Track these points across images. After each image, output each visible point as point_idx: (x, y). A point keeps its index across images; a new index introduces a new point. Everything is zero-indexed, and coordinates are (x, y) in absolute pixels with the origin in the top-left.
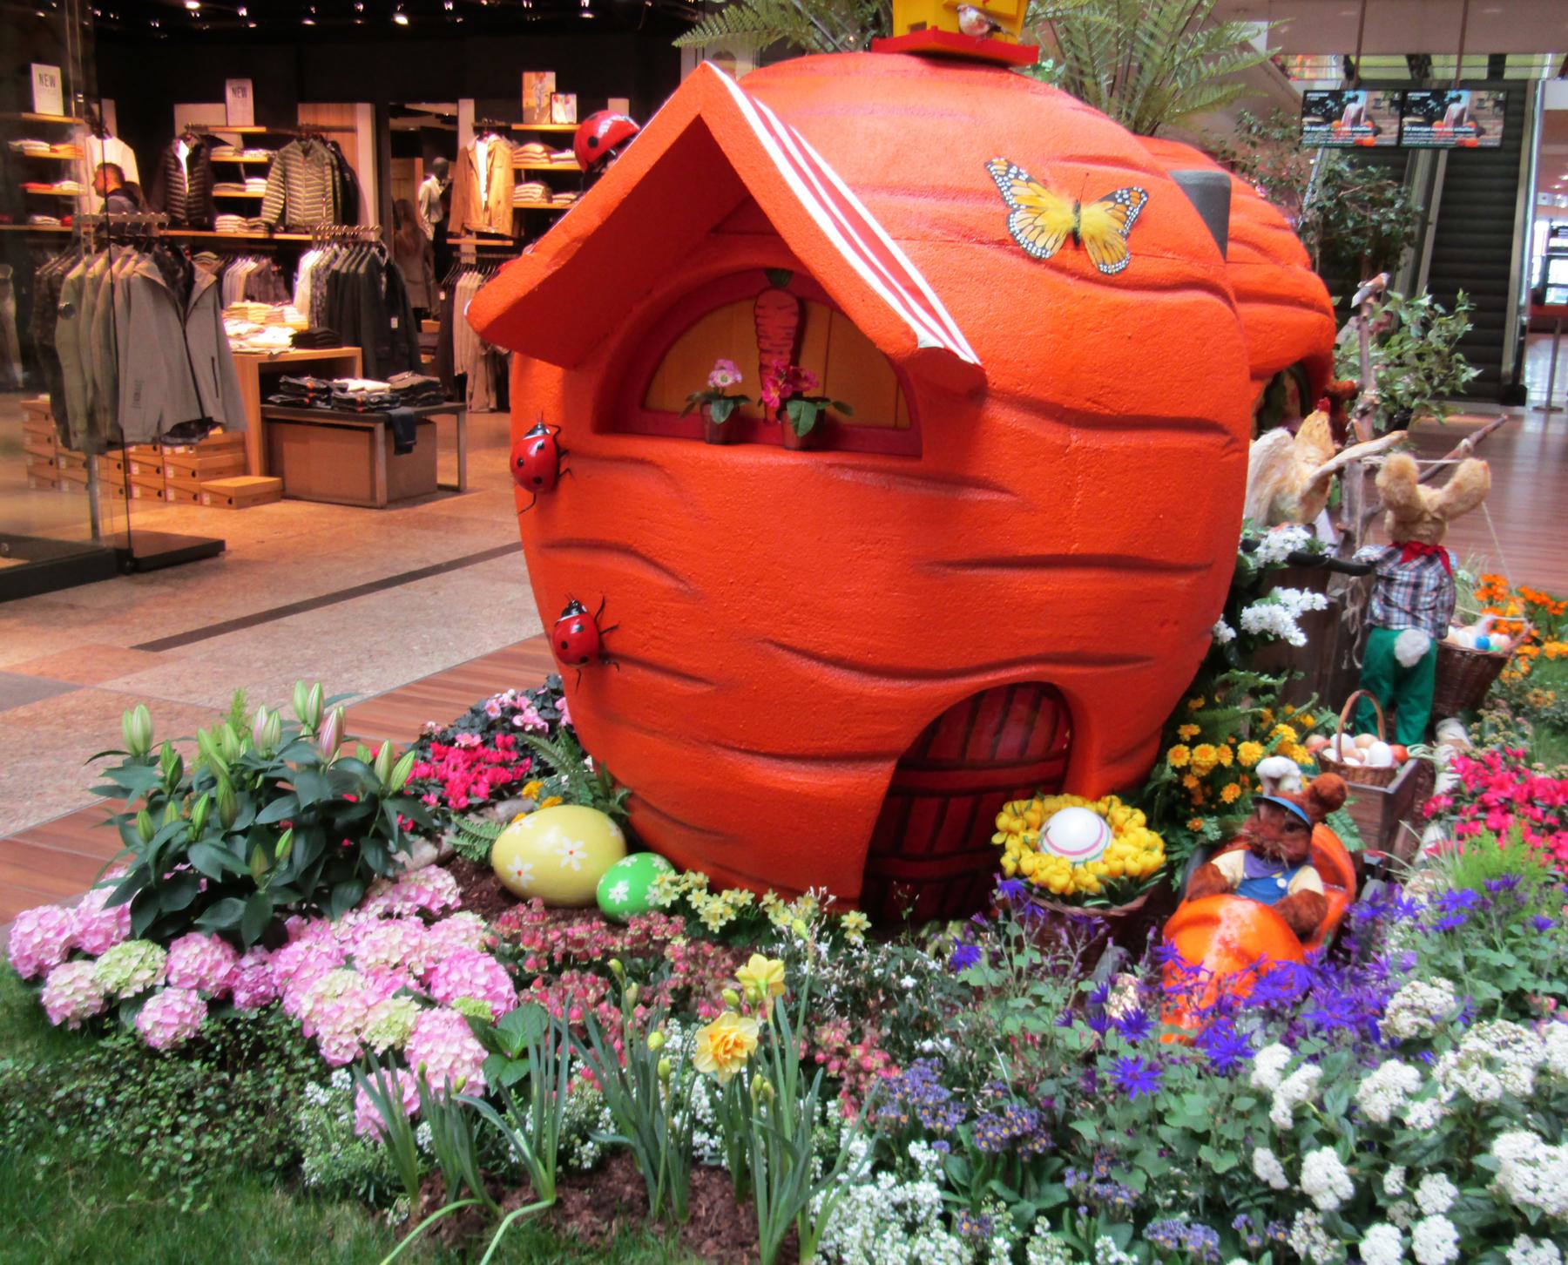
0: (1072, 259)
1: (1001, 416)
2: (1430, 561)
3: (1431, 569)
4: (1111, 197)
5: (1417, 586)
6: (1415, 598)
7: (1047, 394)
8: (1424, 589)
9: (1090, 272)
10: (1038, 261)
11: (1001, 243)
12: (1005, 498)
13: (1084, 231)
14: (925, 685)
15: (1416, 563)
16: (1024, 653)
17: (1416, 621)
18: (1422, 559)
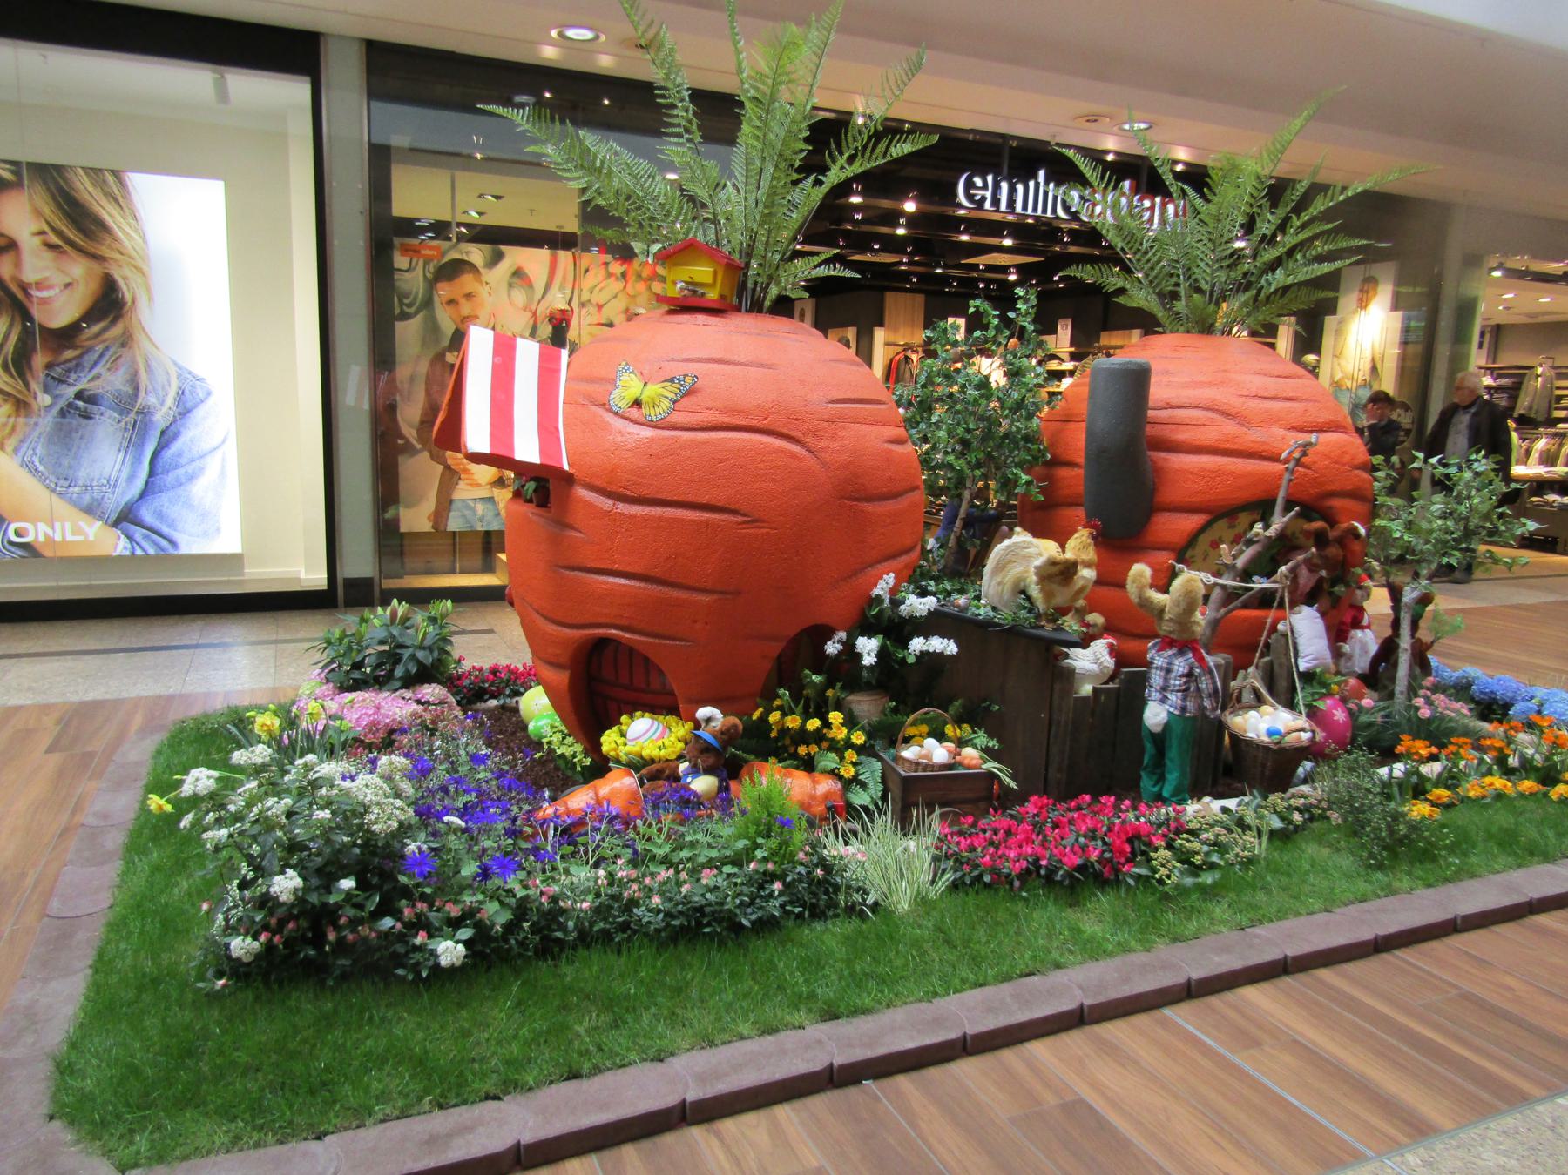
0: (634, 413)
1: (582, 493)
2: (1181, 652)
3: (1181, 660)
4: (671, 380)
5: (1168, 671)
6: (1166, 680)
7: (598, 483)
8: (1173, 675)
9: (642, 420)
10: (616, 414)
11: (604, 405)
12: (579, 535)
13: (644, 398)
14: (559, 628)
15: (1170, 652)
16: (602, 620)
17: (1163, 700)
18: (1174, 650)
